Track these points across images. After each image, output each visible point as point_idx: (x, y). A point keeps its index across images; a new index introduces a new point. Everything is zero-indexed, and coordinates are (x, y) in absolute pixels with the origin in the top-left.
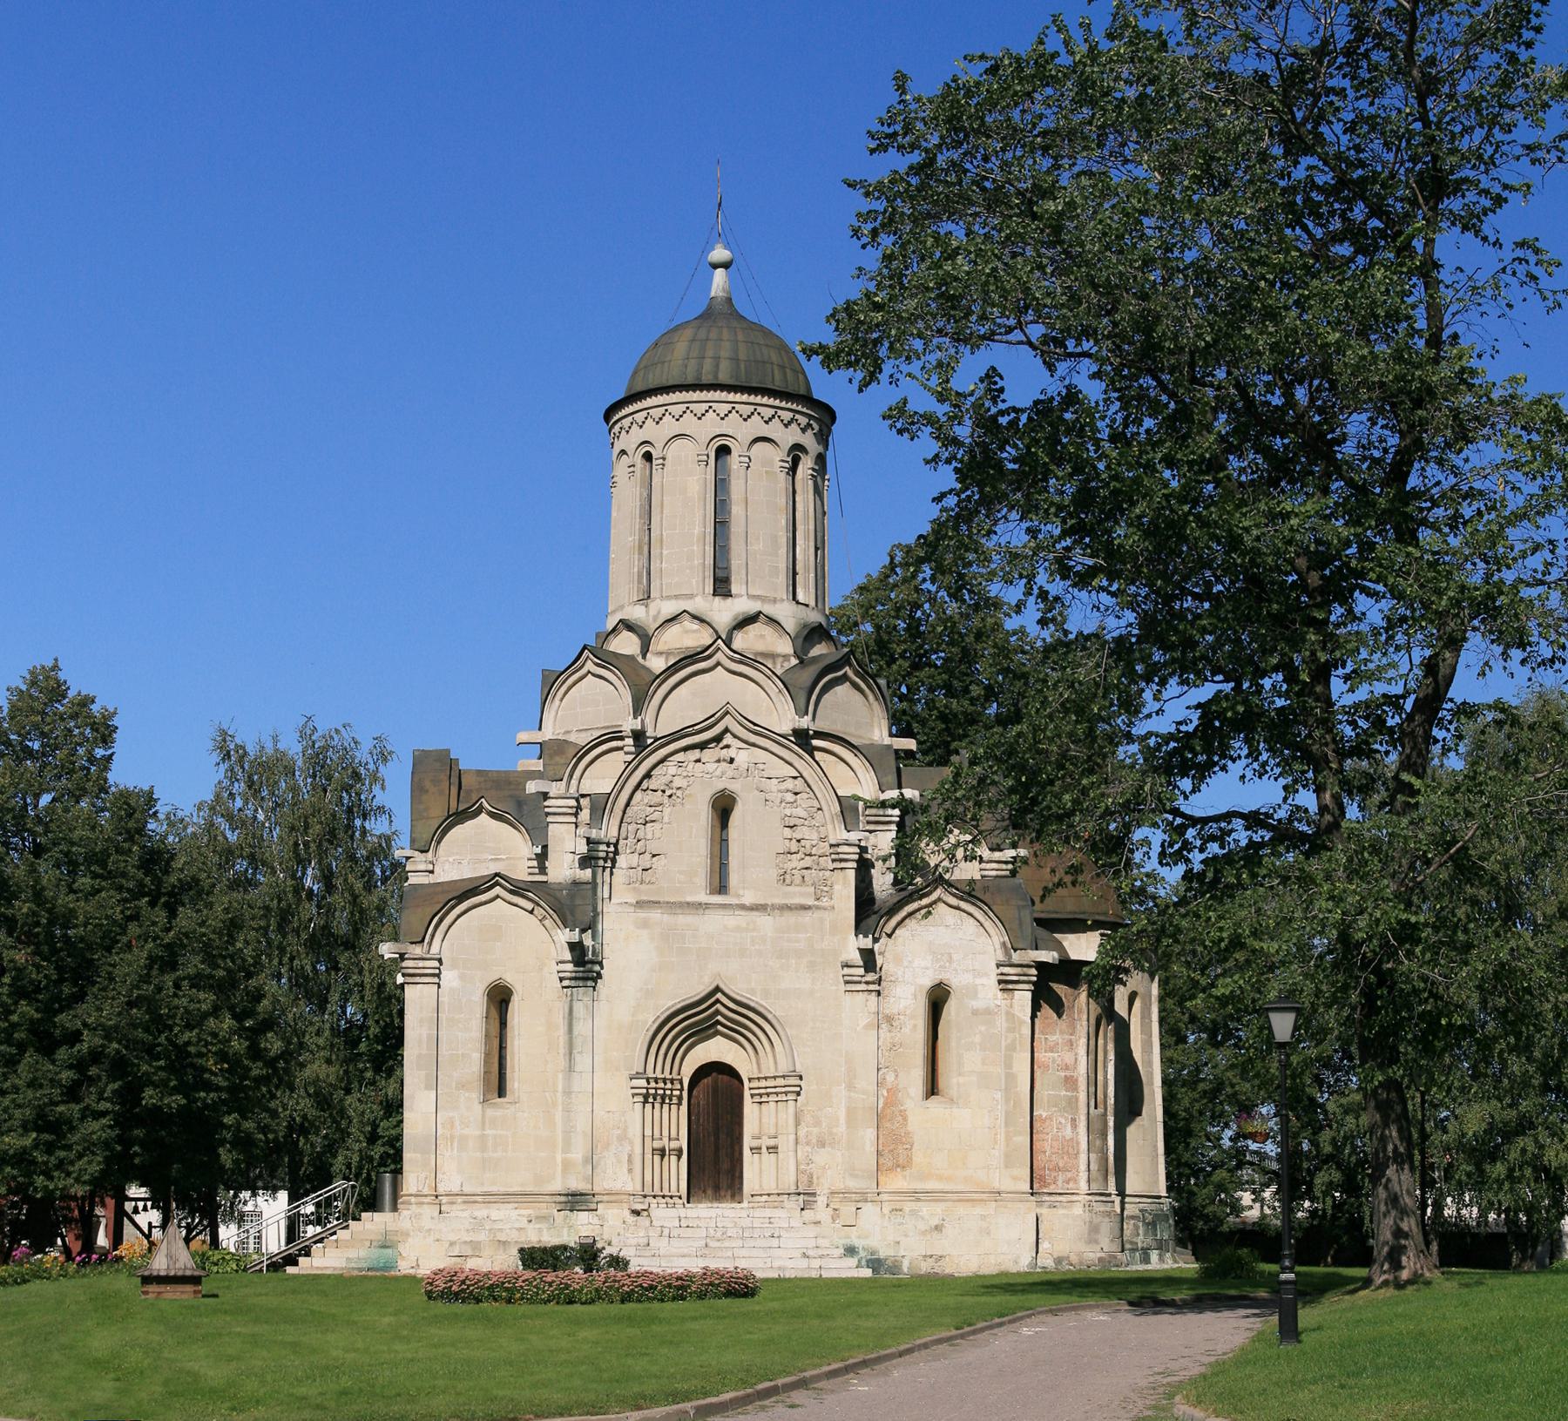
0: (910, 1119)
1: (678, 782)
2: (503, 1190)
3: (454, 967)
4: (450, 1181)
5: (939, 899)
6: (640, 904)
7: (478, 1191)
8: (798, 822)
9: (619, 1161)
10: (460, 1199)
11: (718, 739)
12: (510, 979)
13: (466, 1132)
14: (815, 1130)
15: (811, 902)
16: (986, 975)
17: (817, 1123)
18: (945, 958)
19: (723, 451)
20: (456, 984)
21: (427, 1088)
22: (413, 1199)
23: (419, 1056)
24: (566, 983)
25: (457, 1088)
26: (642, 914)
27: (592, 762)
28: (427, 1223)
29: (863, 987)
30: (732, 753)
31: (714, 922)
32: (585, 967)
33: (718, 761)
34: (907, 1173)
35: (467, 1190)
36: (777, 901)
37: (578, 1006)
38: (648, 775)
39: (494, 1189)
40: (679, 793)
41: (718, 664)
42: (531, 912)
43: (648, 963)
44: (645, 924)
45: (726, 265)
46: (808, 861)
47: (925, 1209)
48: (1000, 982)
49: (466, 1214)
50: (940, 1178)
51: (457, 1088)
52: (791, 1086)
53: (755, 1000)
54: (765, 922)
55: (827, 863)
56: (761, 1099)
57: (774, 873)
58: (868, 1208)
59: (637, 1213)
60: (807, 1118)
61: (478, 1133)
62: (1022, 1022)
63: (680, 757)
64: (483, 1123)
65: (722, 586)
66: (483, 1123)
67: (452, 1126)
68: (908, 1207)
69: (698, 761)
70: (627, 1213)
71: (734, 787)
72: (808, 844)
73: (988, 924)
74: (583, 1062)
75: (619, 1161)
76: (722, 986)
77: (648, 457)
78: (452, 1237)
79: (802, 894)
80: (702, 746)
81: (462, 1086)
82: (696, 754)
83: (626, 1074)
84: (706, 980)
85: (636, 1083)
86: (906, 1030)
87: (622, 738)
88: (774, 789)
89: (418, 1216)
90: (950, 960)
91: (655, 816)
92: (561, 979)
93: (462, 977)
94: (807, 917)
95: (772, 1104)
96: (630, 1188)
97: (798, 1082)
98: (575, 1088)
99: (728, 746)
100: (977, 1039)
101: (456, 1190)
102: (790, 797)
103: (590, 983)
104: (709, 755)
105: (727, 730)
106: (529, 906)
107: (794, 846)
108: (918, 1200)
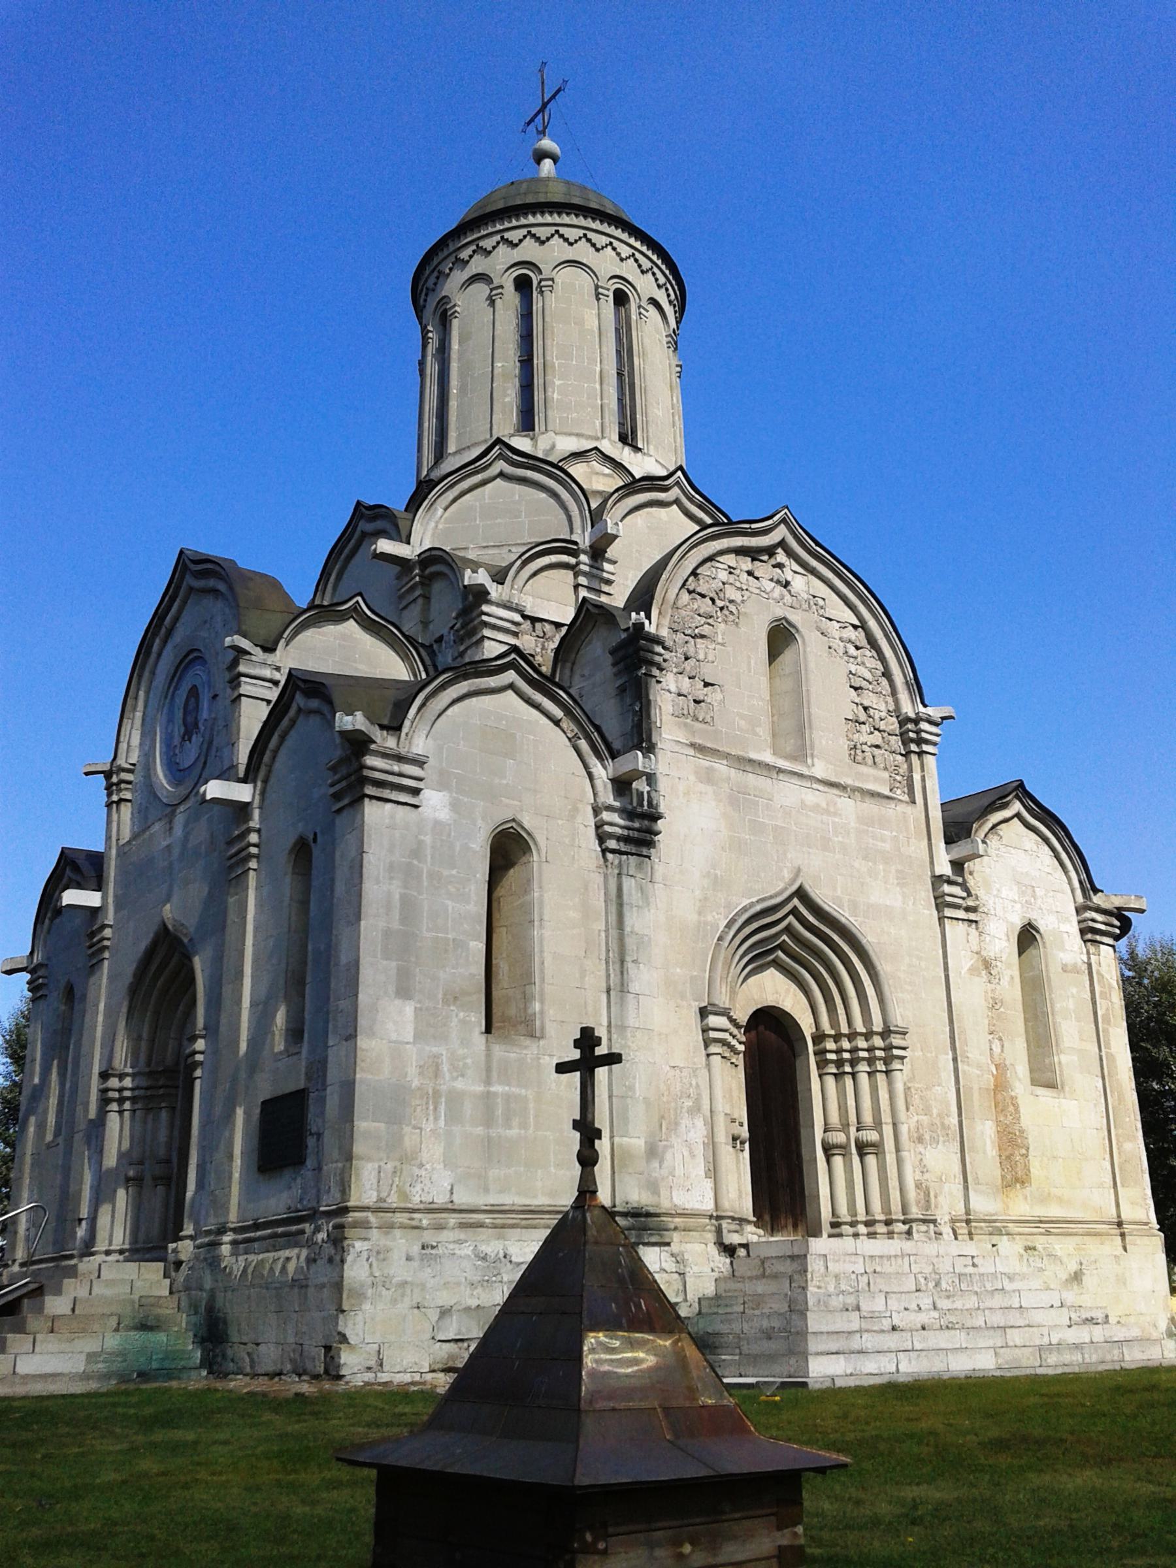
0: (1022, 1110)
1: (731, 593)
2: (520, 1201)
3: (442, 786)
4: (435, 1183)
5: (1018, 815)
6: (700, 749)
7: (481, 1201)
8: (864, 684)
9: (693, 1156)
10: (453, 1219)
11: (770, 551)
12: (528, 821)
13: (459, 1085)
14: (925, 1119)
15: (887, 792)
16: (1067, 920)
17: (927, 1111)
18: (1029, 891)
19: (621, 299)
20: (444, 815)
21: (404, 992)
22: (372, 1218)
23: (387, 933)
24: (612, 844)
25: (446, 1002)
26: (704, 762)
27: (535, 574)
28: (399, 1270)
29: (961, 914)
30: (788, 575)
31: (788, 793)
32: (635, 829)
33: (771, 580)
34: (1027, 1191)
35: (463, 1198)
36: (849, 782)
37: (628, 883)
38: (694, 573)
39: (508, 1200)
40: (732, 608)
41: (677, 501)
42: (557, 723)
43: (720, 838)
44: (708, 777)
45: (555, 160)
46: (877, 738)
47: (1062, 1246)
48: (1083, 932)
49: (467, 1250)
50: (1060, 1200)
51: (446, 1002)
52: (884, 1051)
53: (844, 915)
54: (847, 805)
55: (896, 742)
56: (842, 1068)
57: (845, 745)
58: (1004, 1242)
59: (729, 1250)
60: (916, 1100)
61: (479, 1088)
62: (1111, 987)
63: (730, 559)
64: (488, 1069)
65: (627, 438)
66: (488, 1069)
67: (437, 1073)
68: (1040, 1242)
69: (750, 573)
70: (713, 1250)
71: (795, 617)
72: (877, 717)
73: (1064, 856)
74: (642, 978)
75: (693, 1156)
76: (807, 887)
77: (523, 285)
78: (445, 1298)
79: (876, 779)
80: (753, 554)
81: (453, 998)
82: (746, 564)
83: (696, 1006)
84: (787, 875)
85: (714, 1020)
86: (1005, 981)
87: (574, 553)
88: (837, 635)
89: (381, 1254)
90: (1034, 897)
91: (706, 630)
92: (601, 838)
93: (455, 806)
94: (892, 811)
95: (863, 1079)
96: (708, 1206)
97: (902, 1043)
98: (632, 1021)
99: (780, 566)
100: (1071, 1004)
101: (441, 1199)
102: (852, 650)
103: (645, 851)
104: (762, 569)
105: (782, 544)
106: (558, 713)
107: (862, 716)
108: (1048, 1233)
